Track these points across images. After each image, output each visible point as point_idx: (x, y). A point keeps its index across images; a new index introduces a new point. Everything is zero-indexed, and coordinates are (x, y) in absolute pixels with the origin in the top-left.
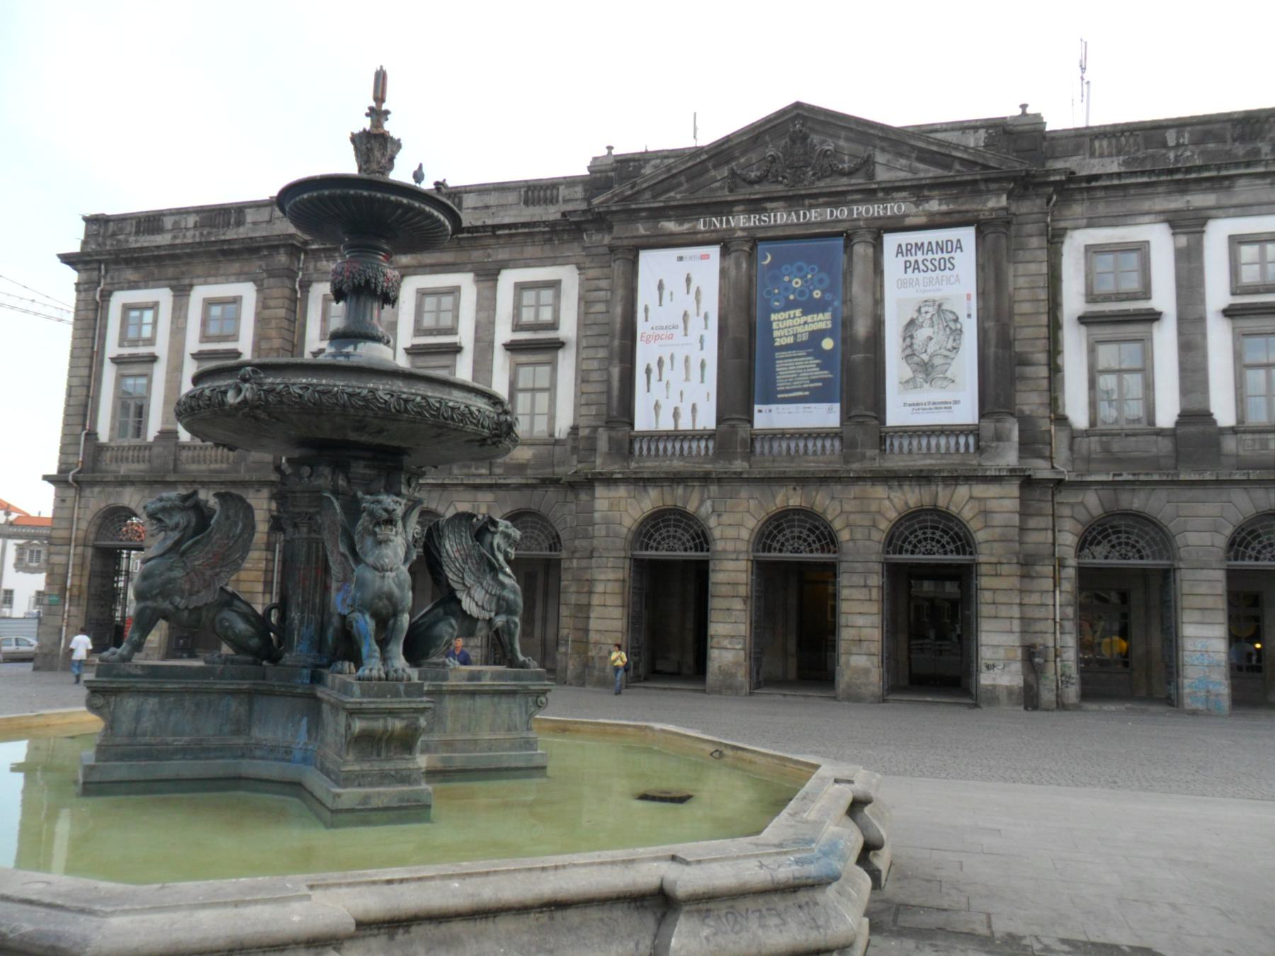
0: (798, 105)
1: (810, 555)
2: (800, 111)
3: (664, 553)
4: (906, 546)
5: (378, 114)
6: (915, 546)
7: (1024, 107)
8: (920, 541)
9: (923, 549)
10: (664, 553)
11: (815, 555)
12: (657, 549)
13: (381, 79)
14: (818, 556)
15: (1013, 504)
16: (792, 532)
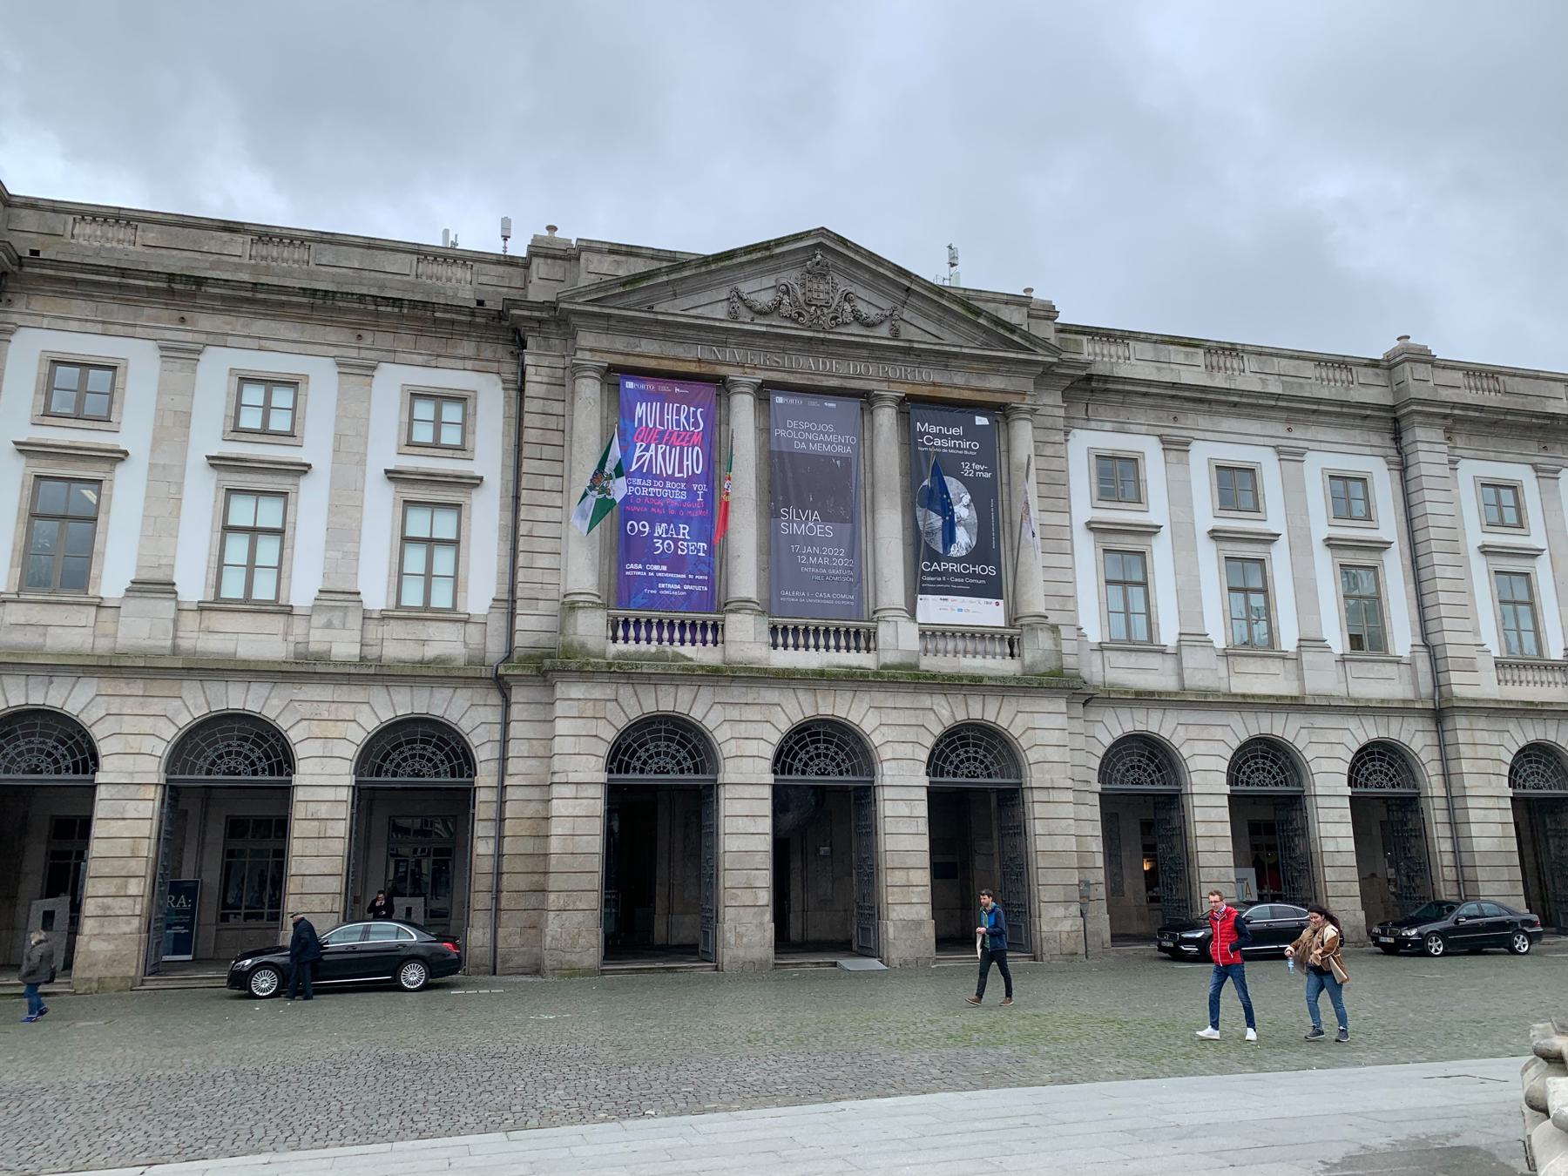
0: (823, 232)
1: (839, 778)
2: (824, 241)
3: (652, 776)
4: (947, 767)
8: (975, 759)
9: (966, 771)
10: (652, 776)
11: (845, 778)
16: (817, 748)
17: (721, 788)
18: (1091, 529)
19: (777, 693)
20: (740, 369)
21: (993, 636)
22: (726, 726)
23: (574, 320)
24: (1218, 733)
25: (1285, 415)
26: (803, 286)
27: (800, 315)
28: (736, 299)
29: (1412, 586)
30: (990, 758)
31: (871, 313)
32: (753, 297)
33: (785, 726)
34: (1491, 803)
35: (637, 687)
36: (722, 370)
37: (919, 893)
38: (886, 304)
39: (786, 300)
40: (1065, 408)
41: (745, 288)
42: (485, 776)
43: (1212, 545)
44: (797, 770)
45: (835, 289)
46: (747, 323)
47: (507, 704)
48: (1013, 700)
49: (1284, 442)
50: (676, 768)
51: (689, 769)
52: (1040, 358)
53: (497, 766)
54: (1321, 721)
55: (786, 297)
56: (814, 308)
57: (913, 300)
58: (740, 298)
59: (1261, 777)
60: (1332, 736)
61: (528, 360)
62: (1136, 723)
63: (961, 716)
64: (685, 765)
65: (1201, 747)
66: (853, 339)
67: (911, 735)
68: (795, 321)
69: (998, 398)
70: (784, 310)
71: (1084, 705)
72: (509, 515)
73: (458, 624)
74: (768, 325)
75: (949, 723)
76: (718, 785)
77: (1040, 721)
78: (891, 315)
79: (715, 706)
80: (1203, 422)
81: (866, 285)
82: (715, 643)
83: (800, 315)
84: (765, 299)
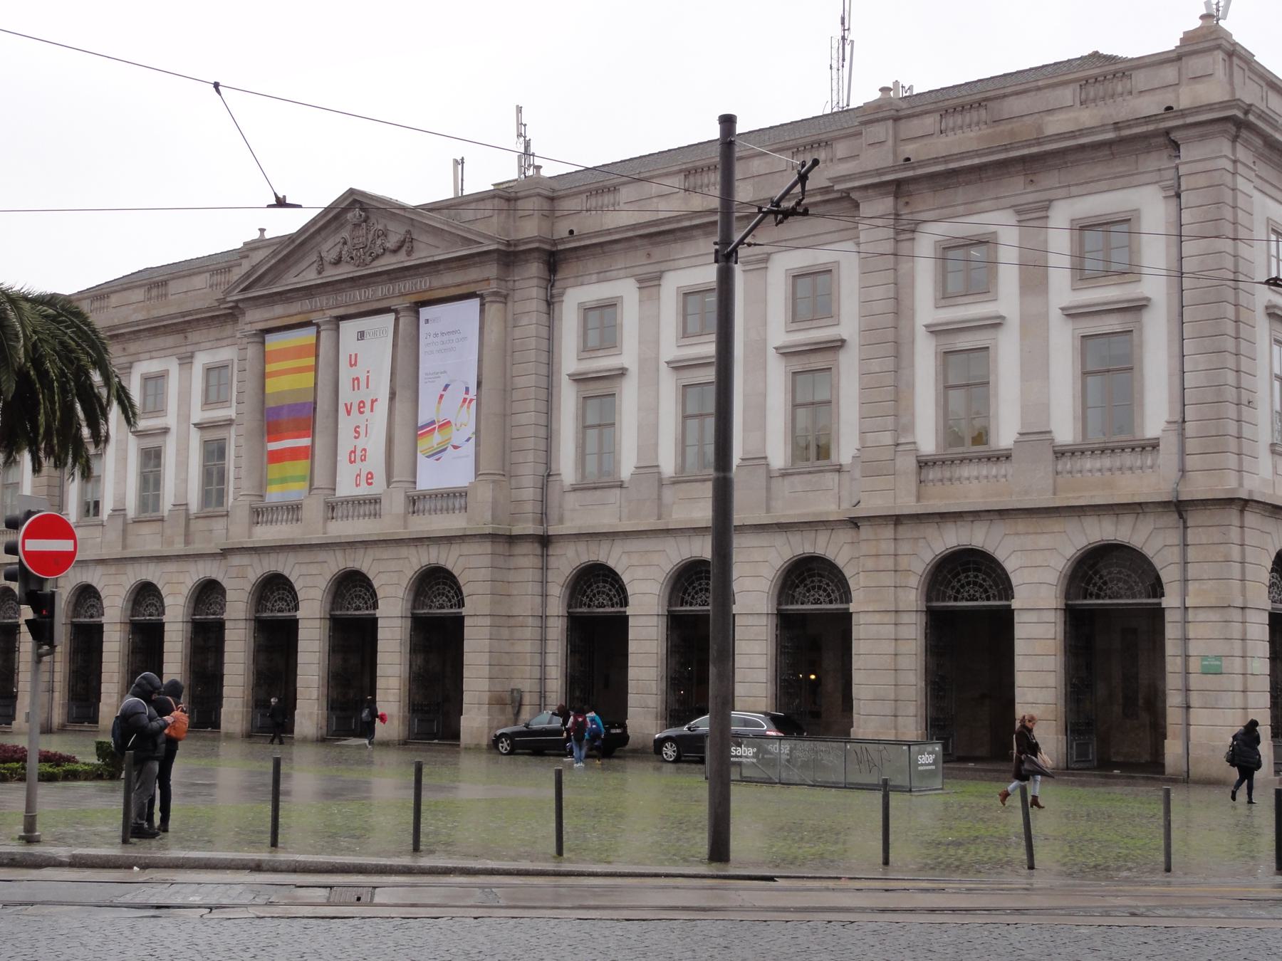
0: (351, 192)
21: (454, 495)
23: (241, 305)
46: (333, 274)
59: (601, 600)
65: (640, 573)
69: (471, 289)
70: (345, 256)
82: (298, 520)
83: (352, 258)
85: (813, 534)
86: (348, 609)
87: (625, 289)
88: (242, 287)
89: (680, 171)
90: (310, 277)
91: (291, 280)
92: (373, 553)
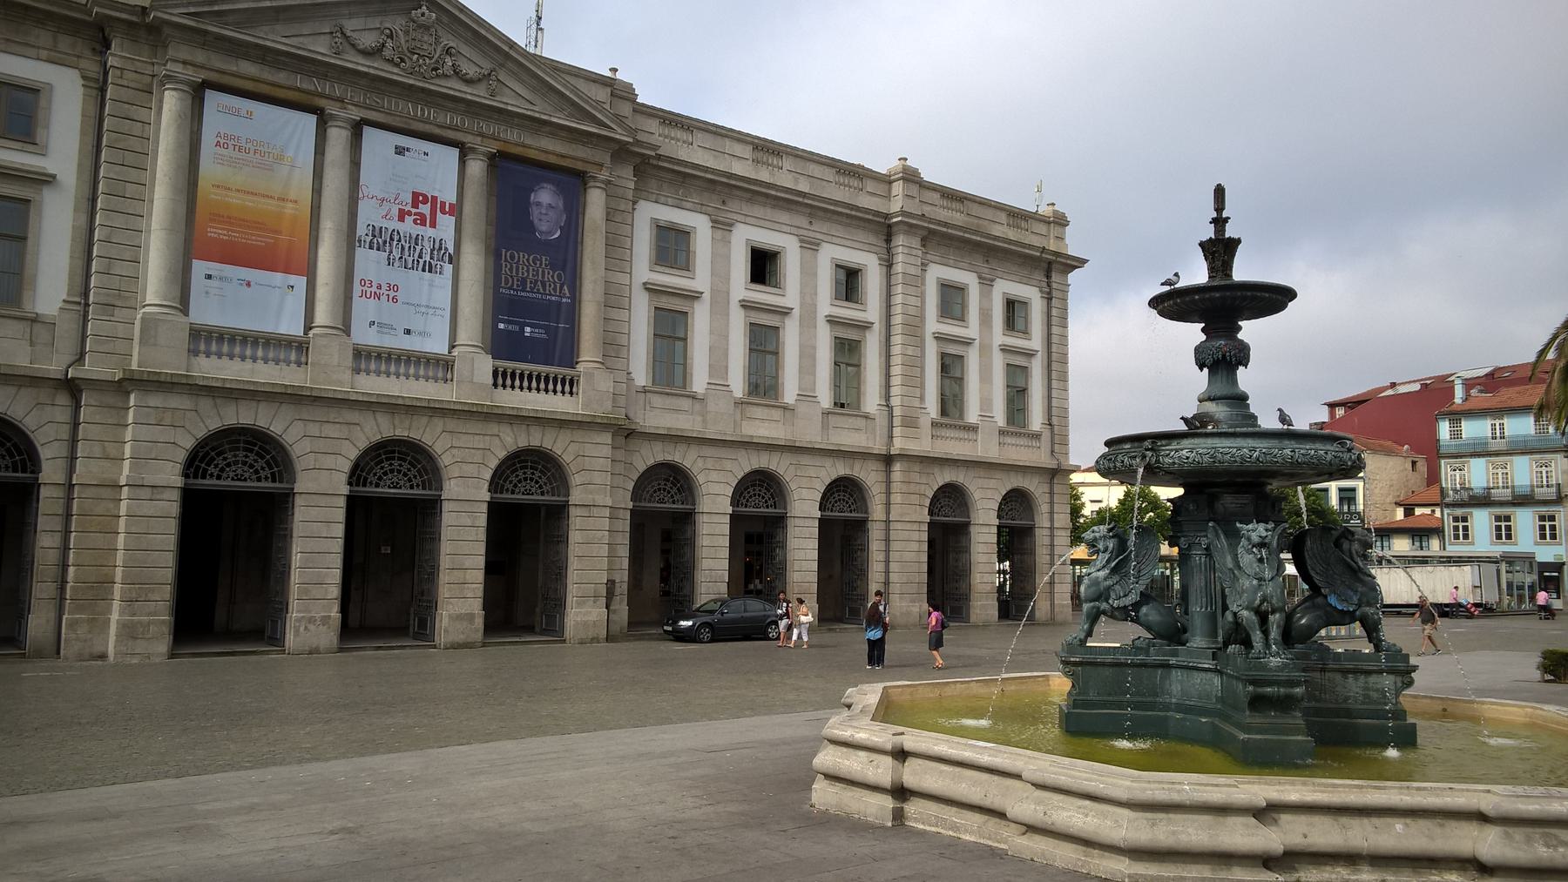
5: (1220, 222)
6: (515, 486)
7: (614, 70)
12: (219, 477)
13: (1219, 193)
14: (266, 485)
15: (607, 451)
17: (297, 496)
18: (646, 289)
19: (357, 413)
20: (339, 104)
22: (307, 441)
24: (728, 465)
25: (809, 211)
26: (407, 33)
27: (402, 60)
28: (339, 35)
29: (883, 359)
30: (544, 479)
31: (470, 70)
32: (354, 35)
33: (363, 444)
34: (908, 526)
35: (219, 401)
36: (322, 103)
37: (474, 589)
38: (487, 65)
39: (389, 44)
40: (636, 182)
41: (350, 25)
42: (51, 472)
43: (742, 312)
44: (371, 483)
45: (437, 42)
47: (78, 407)
48: (568, 432)
49: (805, 233)
50: (254, 477)
51: (266, 478)
52: (618, 137)
53: (65, 465)
54: (806, 459)
55: (389, 40)
56: (416, 56)
57: (510, 64)
58: (342, 33)
59: (757, 501)
60: (812, 472)
61: (111, 61)
62: (666, 454)
63: (523, 443)
64: (262, 474)
65: (714, 476)
66: (452, 92)
67: (478, 457)
68: (397, 65)
69: (579, 166)
70: (387, 53)
71: (626, 437)
72: (83, 219)
73: (25, 322)
74: (369, 67)
75: (512, 448)
76: (294, 494)
77: (590, 450)
78: (490, 74)
79: (295, 422)
80: (746, 209)
81: (467, 42)
83: (402, 60)
84: (368, 40)
85: (852, 461)
86: (377, 485)
87: (698, 223)
88: (192, 10)
89: (752, 143)
90: (320, 48)
91: (275, 38)
92: (439, 424)
